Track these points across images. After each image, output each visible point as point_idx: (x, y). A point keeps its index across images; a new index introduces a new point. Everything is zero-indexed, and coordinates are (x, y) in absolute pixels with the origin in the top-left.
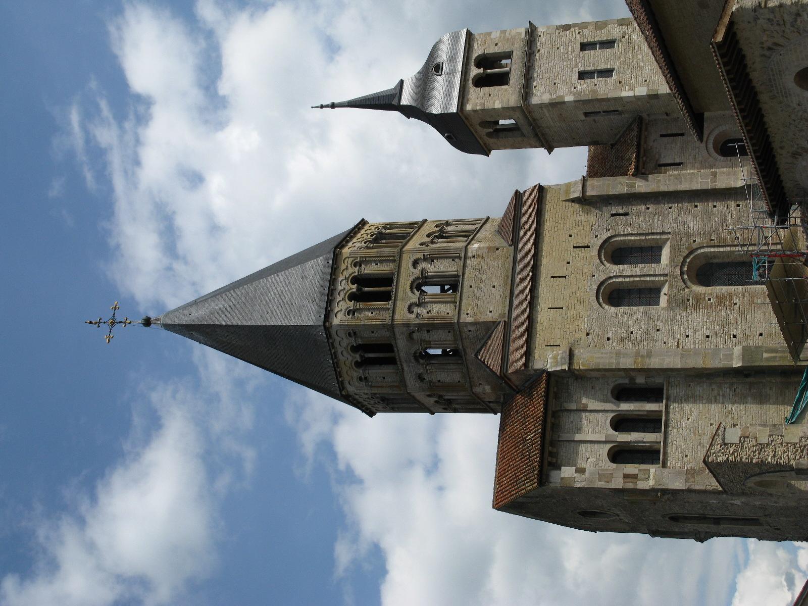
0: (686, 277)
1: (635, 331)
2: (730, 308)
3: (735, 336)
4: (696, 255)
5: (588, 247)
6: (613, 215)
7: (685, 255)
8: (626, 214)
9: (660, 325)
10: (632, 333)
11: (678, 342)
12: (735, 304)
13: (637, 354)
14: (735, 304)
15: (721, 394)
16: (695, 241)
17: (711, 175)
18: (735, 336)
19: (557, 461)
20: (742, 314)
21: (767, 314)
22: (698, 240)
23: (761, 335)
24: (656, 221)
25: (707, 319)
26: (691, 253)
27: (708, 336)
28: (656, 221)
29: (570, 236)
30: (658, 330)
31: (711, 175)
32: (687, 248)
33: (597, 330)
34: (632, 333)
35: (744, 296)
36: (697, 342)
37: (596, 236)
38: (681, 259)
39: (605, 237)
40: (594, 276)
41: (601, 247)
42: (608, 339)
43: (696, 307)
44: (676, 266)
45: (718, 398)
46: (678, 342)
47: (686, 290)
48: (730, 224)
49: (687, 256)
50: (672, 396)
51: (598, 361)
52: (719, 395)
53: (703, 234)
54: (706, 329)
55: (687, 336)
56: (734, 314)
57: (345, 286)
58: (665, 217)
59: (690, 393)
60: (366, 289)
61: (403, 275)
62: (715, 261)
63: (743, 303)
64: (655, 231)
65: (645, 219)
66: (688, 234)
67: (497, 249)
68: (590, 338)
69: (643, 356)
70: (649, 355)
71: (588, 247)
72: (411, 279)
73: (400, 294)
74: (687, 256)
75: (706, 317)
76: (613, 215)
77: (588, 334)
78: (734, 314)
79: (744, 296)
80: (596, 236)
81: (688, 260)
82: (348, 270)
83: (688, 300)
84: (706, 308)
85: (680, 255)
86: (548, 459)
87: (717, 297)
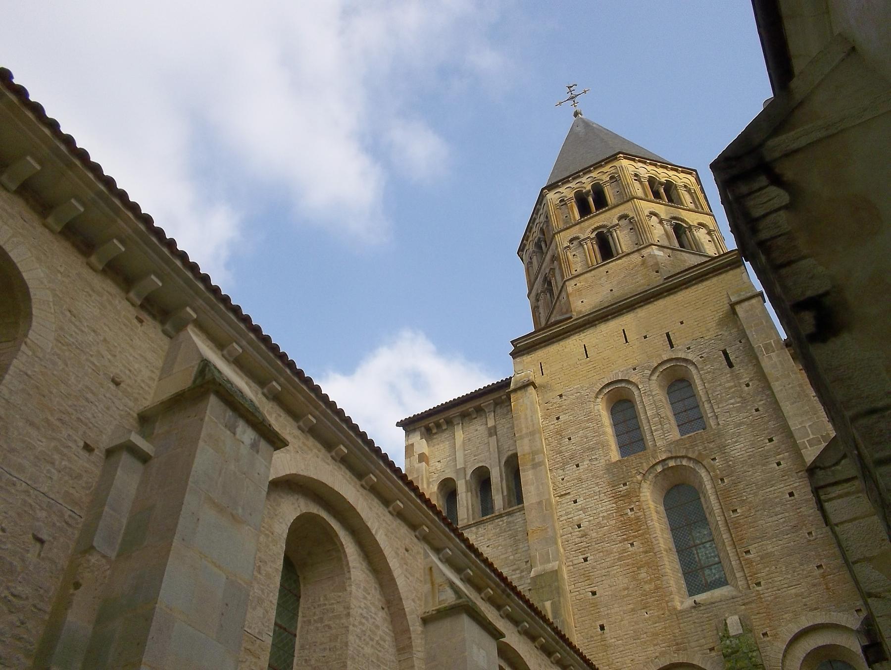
0: (659, 469)
1: (573, 441)
2: (625, 540)
3: (586, 560)
4: (695, 470)
5: (672, 346)
6: (725, 353)
7: (690, 455)
8: (731, 365)
9: (585, 465)
10: (570, 439)
11: (566, 494)
12: (632, 544)
13: (534, 453)
14: (632, 544)
15: (524, 574)
16: (714, 459)
17: (822, 436)
18: (586, 560)
19: (435, 434)
20: (618, 559)
21: (626, 592)
22: (717, 463)
23: (594, 593)
24: (732, 401)
25: (604, 517)
26: (696, 461)
27: (579, 526)
28: (732, 401)
29: (682, 323)
30: (577, 466)
31: (822, 436)
32: (700, 454)
33: (567, 402)
34: (570, 439)
35: (646, 552)
36: (569, 516)
37: (689, 348)
38: (683, 453)
39: (690, 357)
40: (635, 369)
41: (677, 359)
42: (558, 418)
43: (617, 497)
44: (670, 452)
45: (518, 572)
46: (566, 494)
47: (639, 477)
48: (755, 494)
49: (690, 459)
50: (514, 518)
51: (523, 416)
52: (522, 571)
53: (729, 466)
54: (589, 521)
55: (575, 502)
56: (616, 548)
57: (586, 183)
58: (739, 410)
59: (519, 537)
60: (591, 200)
61: (608, 214)
62: (702, 500)
63: (635, 553)
64: (715, 407)
65: (730, 388)
66: (722, 448)
67: (657, 272)
68: (558, 400)
69: (533, 459)
70: (536, 466)
71: (672, 346)
72: (605, 223)
73: (586, 224)
74: (690, 459)
75: (605, 514)
76: (725, 353)
77: (561, 396)
78: (616, 548)
79: (646, 552)
80: (689, 348)
81: (684, 462)
82: (601, 175)
83: (625, 484)
84: (618, 509)
85: (687, 449)
86: (431, 422)
87: (638, 518)
